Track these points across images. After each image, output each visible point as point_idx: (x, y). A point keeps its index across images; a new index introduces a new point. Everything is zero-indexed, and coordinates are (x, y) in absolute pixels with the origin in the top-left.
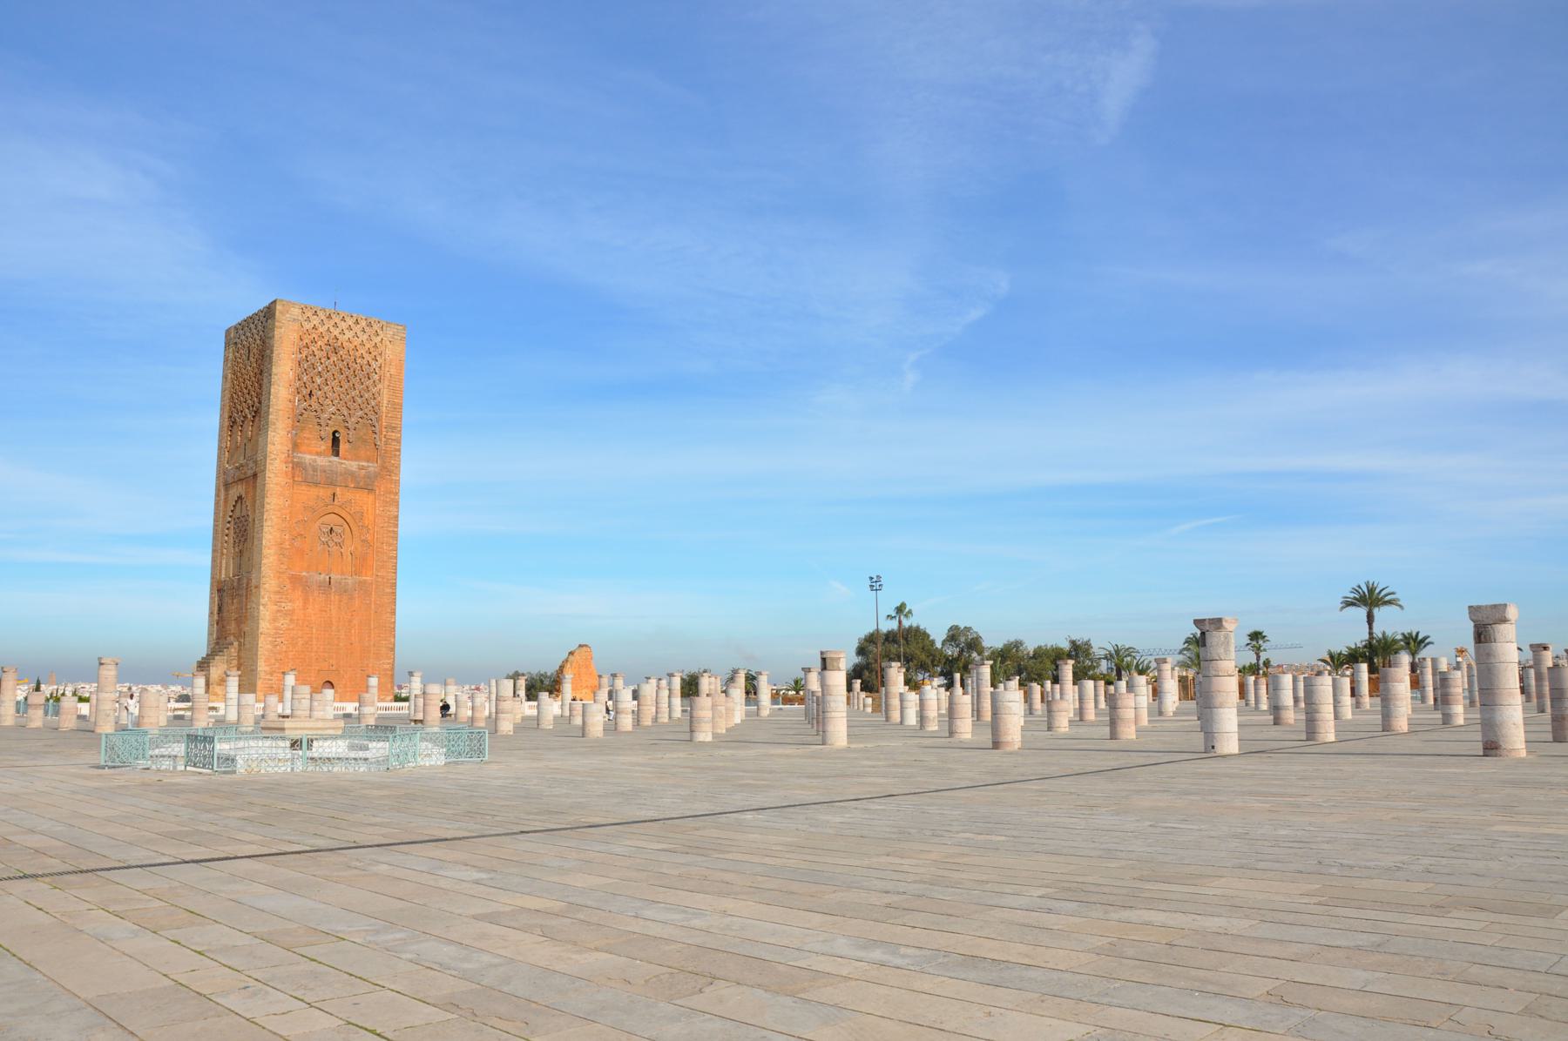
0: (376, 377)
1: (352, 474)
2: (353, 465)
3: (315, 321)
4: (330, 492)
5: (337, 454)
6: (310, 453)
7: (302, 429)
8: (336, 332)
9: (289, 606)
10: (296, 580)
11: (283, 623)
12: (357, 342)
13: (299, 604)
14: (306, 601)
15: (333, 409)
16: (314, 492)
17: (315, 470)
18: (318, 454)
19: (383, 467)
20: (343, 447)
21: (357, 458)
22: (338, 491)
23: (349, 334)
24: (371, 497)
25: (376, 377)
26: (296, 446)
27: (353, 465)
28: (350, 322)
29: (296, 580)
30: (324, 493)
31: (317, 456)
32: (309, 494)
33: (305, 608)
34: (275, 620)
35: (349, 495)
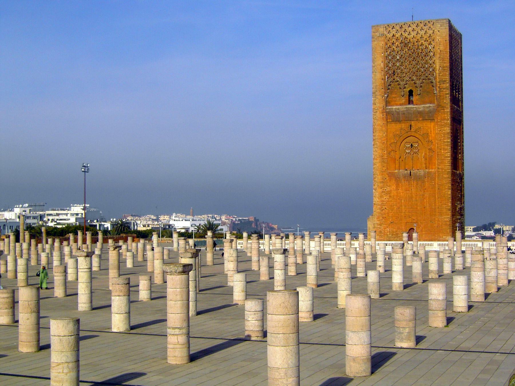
0: (432, 54)
1: (420, 113)
3: (393, 32)
4: (408, 125)
5: (410, 102)
6: (397, 105)
7: (391, 93)
8: (406, 35)
9: (388, 189)
10: (391, 175)
11: (386, 198)
12: (419, 36)
13: (394, 187)
15: (408, 79)
16: (398, 126)
17: (398, 113)
18: (401, 105)
19: (439, 106)
20: (414, 98)
21: (424, 103)
22: (413, 123)
23: (413, 34)
24: (432, 124)
25: (432, 54)
26: (387, 103)
27: (421, 107)
28: (414, 26)
29: (391, 175)
30: (404, 126)
31: (399, 106)
32: (395, 127)
33: (397, 189)
34: (381, 197)
35: (419, 125)
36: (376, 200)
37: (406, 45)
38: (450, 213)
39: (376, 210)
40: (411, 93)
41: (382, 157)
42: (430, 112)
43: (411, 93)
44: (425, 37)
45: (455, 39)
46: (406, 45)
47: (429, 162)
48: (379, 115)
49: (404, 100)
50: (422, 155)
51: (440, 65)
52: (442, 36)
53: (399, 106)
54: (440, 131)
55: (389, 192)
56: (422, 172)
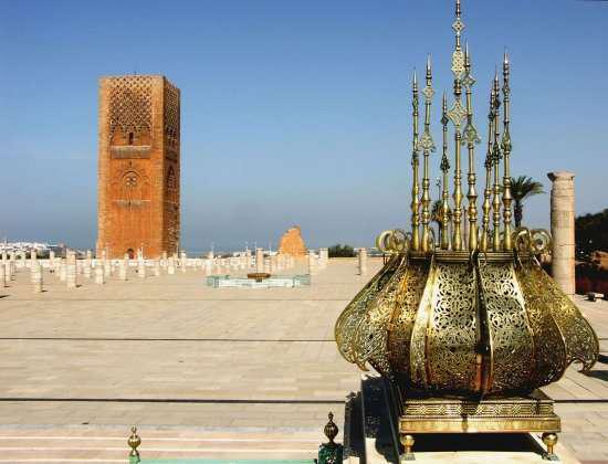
1: (139, 152)
2: (139, 148)
5: (131, 143)
8: (128, 86)
9: (110, 216)
10: (114, 204)
14: (119, 213)
16: (120, 162)
19: (154, 147)
26: (112, 143)
27: (139, 148)
31: (122, 147)
33: (119, 217)
35: (138, 162)
36: (101, 225)
37: (128, 95)
38: (161, 236)
39: (101, 233)
40: (131, 135)
41: (106, 189)
42: (146, 152)
43: (131, 135)
44: (144, 89)
45: (171, 96)
46: (128, 95)
47: (145, 194)
48: (104, 153)
49: (125, 141)
50: (140, 185)
51: (155, 112)
52: (157, 87)
53: (122, 147)
54: (155, 168)
55: (112, 219)
56: (139, 202)
